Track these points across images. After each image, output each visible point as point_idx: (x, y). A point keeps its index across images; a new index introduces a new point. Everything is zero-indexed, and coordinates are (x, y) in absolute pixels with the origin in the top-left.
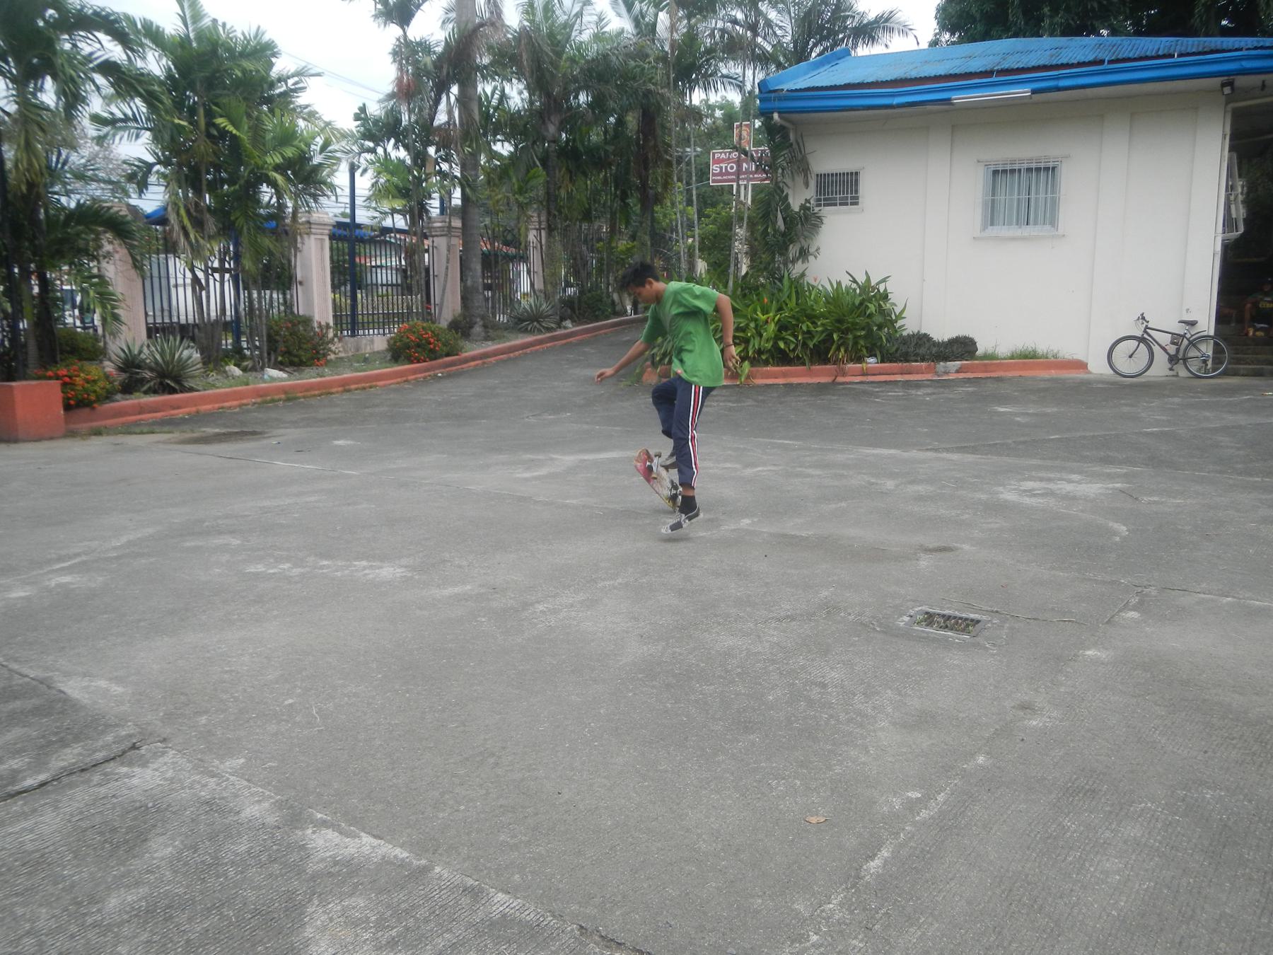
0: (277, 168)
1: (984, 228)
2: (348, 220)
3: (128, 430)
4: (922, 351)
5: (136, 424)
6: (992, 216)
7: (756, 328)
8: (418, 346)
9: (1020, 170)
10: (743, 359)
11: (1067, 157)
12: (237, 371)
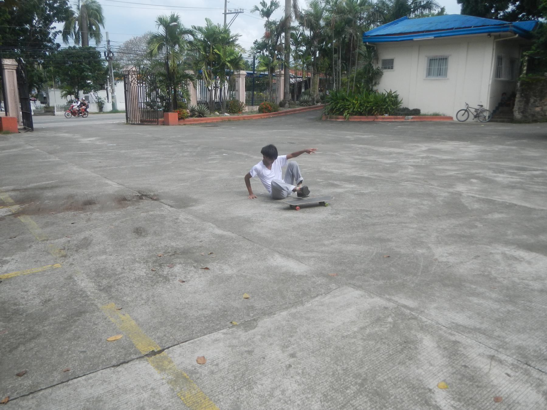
0: (229, 62)
1: (426, 77)
2: (252, 72)
3: (191, 124)
4: (401, 113)
5: (193, 123)
6: (429, 73)
7: (353, 105)
8: (266, 108)
9: (437, 59)
10: (348, 114)
11: (451, 55)
12: (217, 113)
